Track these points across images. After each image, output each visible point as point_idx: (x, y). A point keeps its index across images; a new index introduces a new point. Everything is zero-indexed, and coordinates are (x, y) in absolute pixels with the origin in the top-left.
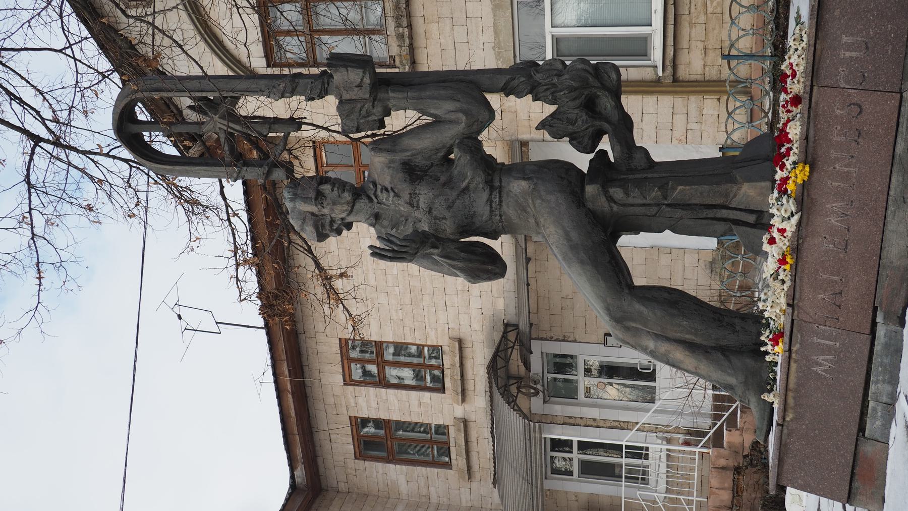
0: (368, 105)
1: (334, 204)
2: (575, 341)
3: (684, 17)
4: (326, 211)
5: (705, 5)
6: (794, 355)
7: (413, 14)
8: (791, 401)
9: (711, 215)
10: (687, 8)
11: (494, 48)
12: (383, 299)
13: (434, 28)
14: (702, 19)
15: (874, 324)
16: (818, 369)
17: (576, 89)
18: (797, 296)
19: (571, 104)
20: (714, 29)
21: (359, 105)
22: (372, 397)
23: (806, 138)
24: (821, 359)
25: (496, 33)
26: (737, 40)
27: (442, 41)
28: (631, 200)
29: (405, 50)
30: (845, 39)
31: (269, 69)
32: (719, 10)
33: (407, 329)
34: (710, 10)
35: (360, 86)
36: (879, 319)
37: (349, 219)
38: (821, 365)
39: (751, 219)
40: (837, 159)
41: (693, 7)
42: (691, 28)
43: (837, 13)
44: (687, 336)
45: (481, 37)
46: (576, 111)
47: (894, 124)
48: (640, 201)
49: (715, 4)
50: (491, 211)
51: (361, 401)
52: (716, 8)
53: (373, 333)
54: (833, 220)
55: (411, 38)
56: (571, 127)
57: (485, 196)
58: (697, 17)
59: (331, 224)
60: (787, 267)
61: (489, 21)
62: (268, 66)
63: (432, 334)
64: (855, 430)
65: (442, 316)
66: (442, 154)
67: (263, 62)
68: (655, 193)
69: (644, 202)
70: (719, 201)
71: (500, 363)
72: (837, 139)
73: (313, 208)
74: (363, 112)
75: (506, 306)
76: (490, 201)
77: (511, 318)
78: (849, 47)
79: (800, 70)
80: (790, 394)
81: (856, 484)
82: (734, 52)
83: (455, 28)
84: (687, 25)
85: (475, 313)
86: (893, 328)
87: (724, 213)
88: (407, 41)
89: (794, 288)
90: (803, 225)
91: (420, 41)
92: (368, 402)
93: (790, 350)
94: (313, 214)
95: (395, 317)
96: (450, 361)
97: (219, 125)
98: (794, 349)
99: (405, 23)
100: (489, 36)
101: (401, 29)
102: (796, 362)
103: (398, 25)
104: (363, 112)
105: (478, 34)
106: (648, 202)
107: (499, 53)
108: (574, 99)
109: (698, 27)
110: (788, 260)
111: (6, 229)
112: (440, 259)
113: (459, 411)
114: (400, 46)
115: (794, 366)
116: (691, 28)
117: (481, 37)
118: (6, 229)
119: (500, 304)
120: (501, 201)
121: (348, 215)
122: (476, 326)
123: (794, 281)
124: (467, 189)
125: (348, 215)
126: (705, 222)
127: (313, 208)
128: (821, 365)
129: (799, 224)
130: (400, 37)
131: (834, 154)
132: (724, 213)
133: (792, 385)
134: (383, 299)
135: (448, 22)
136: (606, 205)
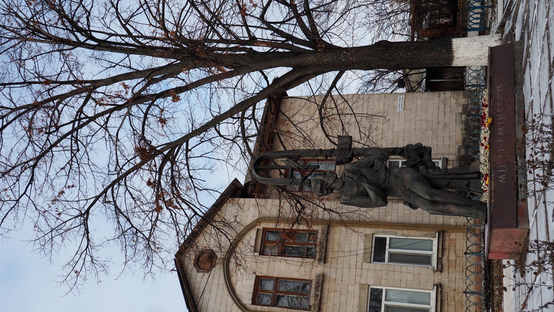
0: (347, 152)
1: (330, 177)
3: (445, 301)
4: (326, 179)
5: (454, 297)
6: (492, 179)
7: (324, 288)
8: (493, 195)
9: (462, 177)
10: (446, 297)
11: (358, 307)
13: (332, 295)
14: (453, 303)
15: (517, 160)
16: (501, 181)
17: (417, 149)
18: (492, 159)
19: (416, 154)
20: (458, 308)
21: (344, 151)
23: (490, 112)
24: (501, 177)
25: (359, 300)
26: (470, 285)
27: (335, 301)
28: (435, 173)
29: (318, 301)
30: (498, 87)
31: (252, 305)
32: (461, 300)
34: (457, 299)
35: (347, 143)
36: (518, 158)
37: (334, 185)
38: (502, 179)
39: (476, 175)
40: (499, 117)
41: (449, 297)
42: (448, 307)
43: (495, 82)
44: (455, 201)
45: (352, 301)
46: (417, 157)
47: (514, 104)
48: (438, 173)
49: (459, 297)
50: (386, 178)
52: (459, 299)
54: (500, 133)
55: (321, 298)
56: (414, 162)
57: (384, 172)
58: (451, 302)
59: (326, 186)
60: (488, 149)
61: (357, 294)
62: (252, 304)
64: (516, 198)
66: (370, 165)
67: (250, 302)
69: (440, 174)
70: (465, 172)
72: (498, 111)
73: (322, 178)
74: (345, 155)
76: (386, 174)
78: (499, 89)
79: (487, 99)
80: (492, 193)
81: (518, 218)
82: (468, 290)
83: (342, 296)
84: (446, 305)
86: (523, 160)
87: (467, 176)
88: (319, 297)
89: (490, 155)
90: (492, 136)
91: (325, 300)
93: (491, 176)
94: (321, 180)
97: (291, 165)
98: (492, 176)
99: (320, 289)
100: (356, 301)
101: (317, 292)
102: (493, 180)
103: (317, 290)
104: (345, 155)
105: (351, 300)
106: (441, 173)
107: (360, 309)
108: (416, 152)
109: (451, 306)
110: (488, 146)
111: (218, 160)
112: (367, 185)
114: (315, 300)
115: (493, 182)
116: (448, 307)
117: (352, 301)
118: (218, 160)
120: (389, 175)
121: (333, 183)
123: (490, 153)
124: (378, 171)
125: (333, 183)
126: (460, 180)
127: (322, 178)
128: (502, 179)
129: (490, 135)
130: (316, 296)
131: (498, 115)
132: (467, 176)
133: (492, 189)
135: (339, 293)
136: (426, 173)
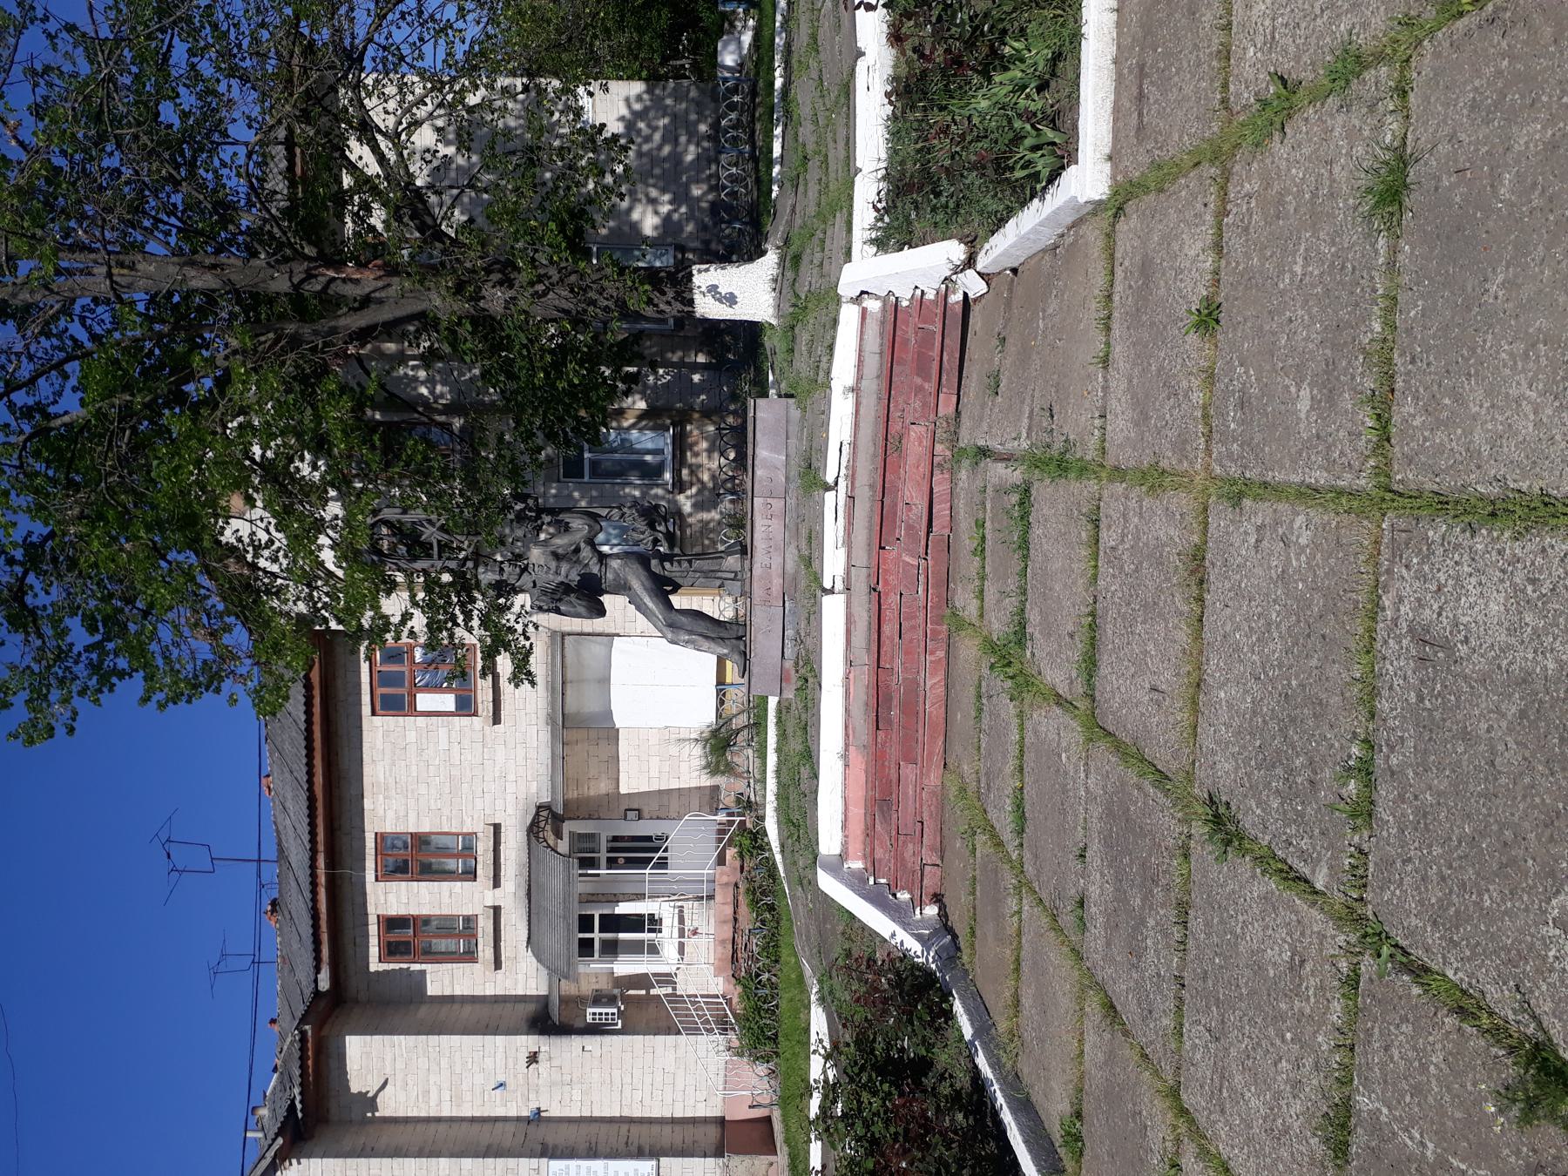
2: (599, 819)
12: (423, 790)
22: (404, 892)
33: (444, 818)
51: (392, 898)
53: (410, 825)
63: (468, 821)
65: (478, 802)
68: (685, 565)
71: (535, 829)
75: (539, 790)
77: (545, 798)
85: (510, 798)
92: (398, 897)
95: (433, 807)
96: (484, 848)
113: (491, 897)
119: (534, 788)
122: (510, 811)
134: (423, 790)
